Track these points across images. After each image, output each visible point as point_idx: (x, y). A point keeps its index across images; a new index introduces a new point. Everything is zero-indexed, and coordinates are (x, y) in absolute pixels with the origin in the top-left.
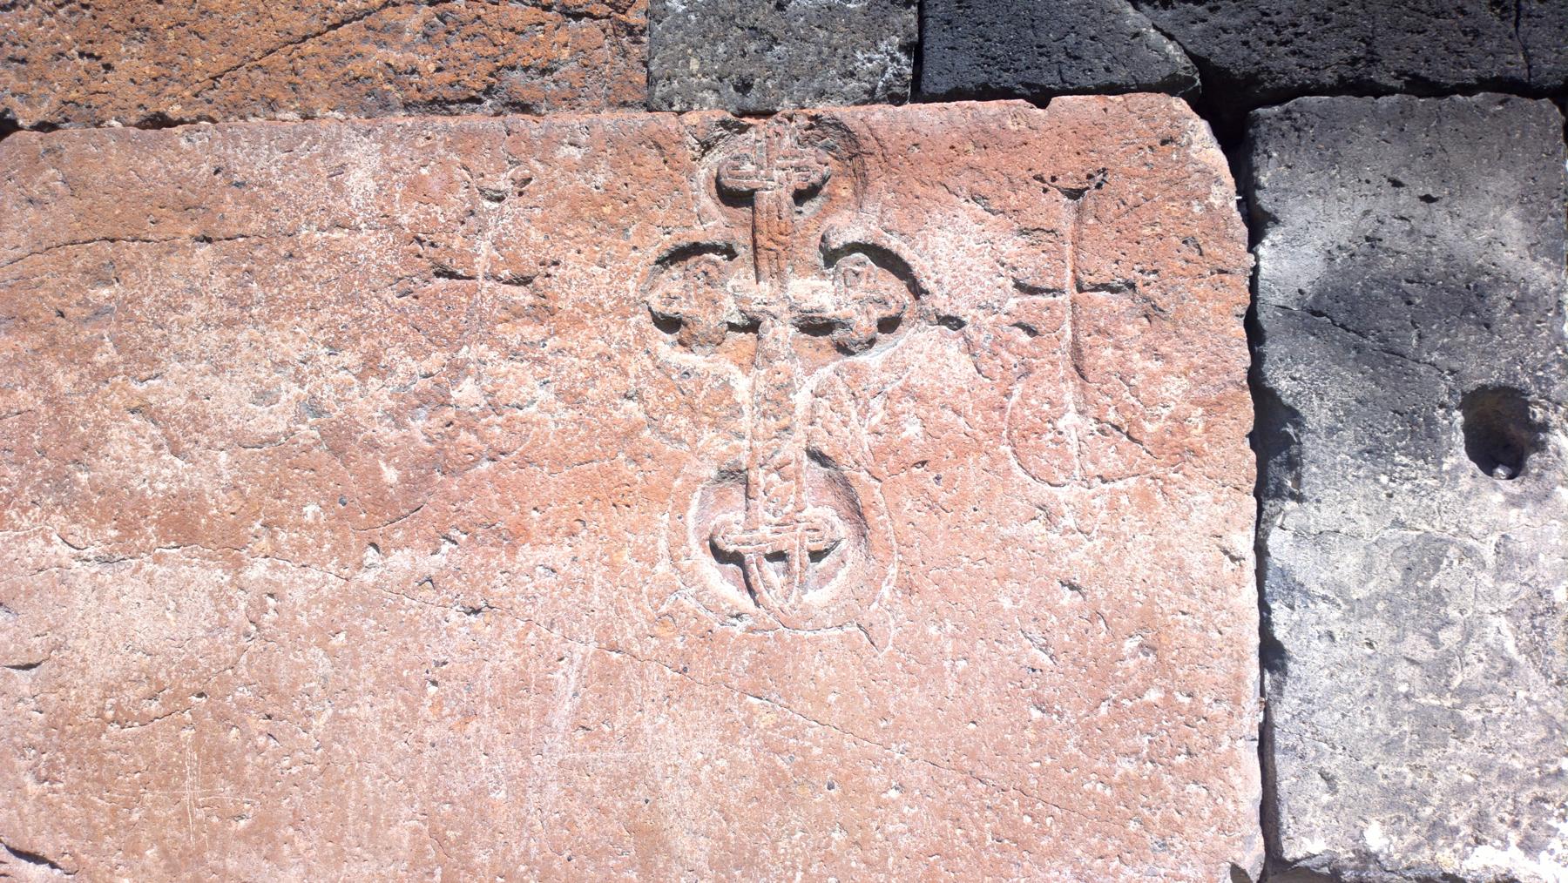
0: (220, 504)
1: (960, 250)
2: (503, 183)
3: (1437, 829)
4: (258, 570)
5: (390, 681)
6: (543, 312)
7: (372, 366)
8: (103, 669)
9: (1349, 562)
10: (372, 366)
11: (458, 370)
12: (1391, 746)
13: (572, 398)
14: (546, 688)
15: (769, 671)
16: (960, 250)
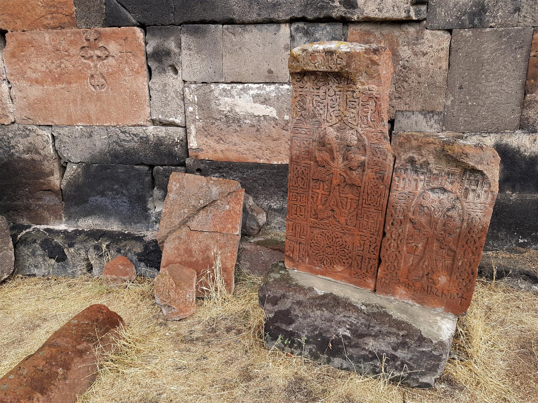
0: (40, 79)
1: (113, 47)
2: (62, 39)
3: (167, 116)
4: (45, 87)
5: (61, 99)
6: (69, 55)
7: (52, 62)
8: (33, 98)
9: (157, 86)
10: (52, 62)
11: (61, 63)
12: (162, 107)
13: (74, 66)
14: (76, 100)
15: (99, 99)
16: (113, 47)
